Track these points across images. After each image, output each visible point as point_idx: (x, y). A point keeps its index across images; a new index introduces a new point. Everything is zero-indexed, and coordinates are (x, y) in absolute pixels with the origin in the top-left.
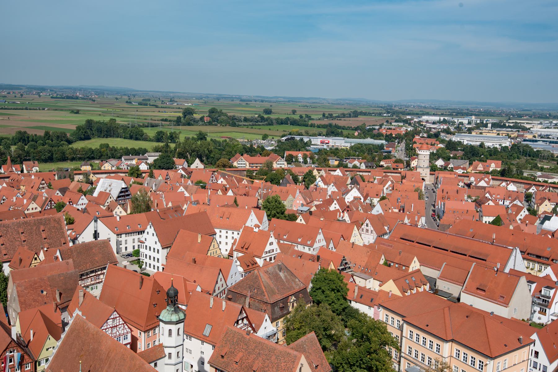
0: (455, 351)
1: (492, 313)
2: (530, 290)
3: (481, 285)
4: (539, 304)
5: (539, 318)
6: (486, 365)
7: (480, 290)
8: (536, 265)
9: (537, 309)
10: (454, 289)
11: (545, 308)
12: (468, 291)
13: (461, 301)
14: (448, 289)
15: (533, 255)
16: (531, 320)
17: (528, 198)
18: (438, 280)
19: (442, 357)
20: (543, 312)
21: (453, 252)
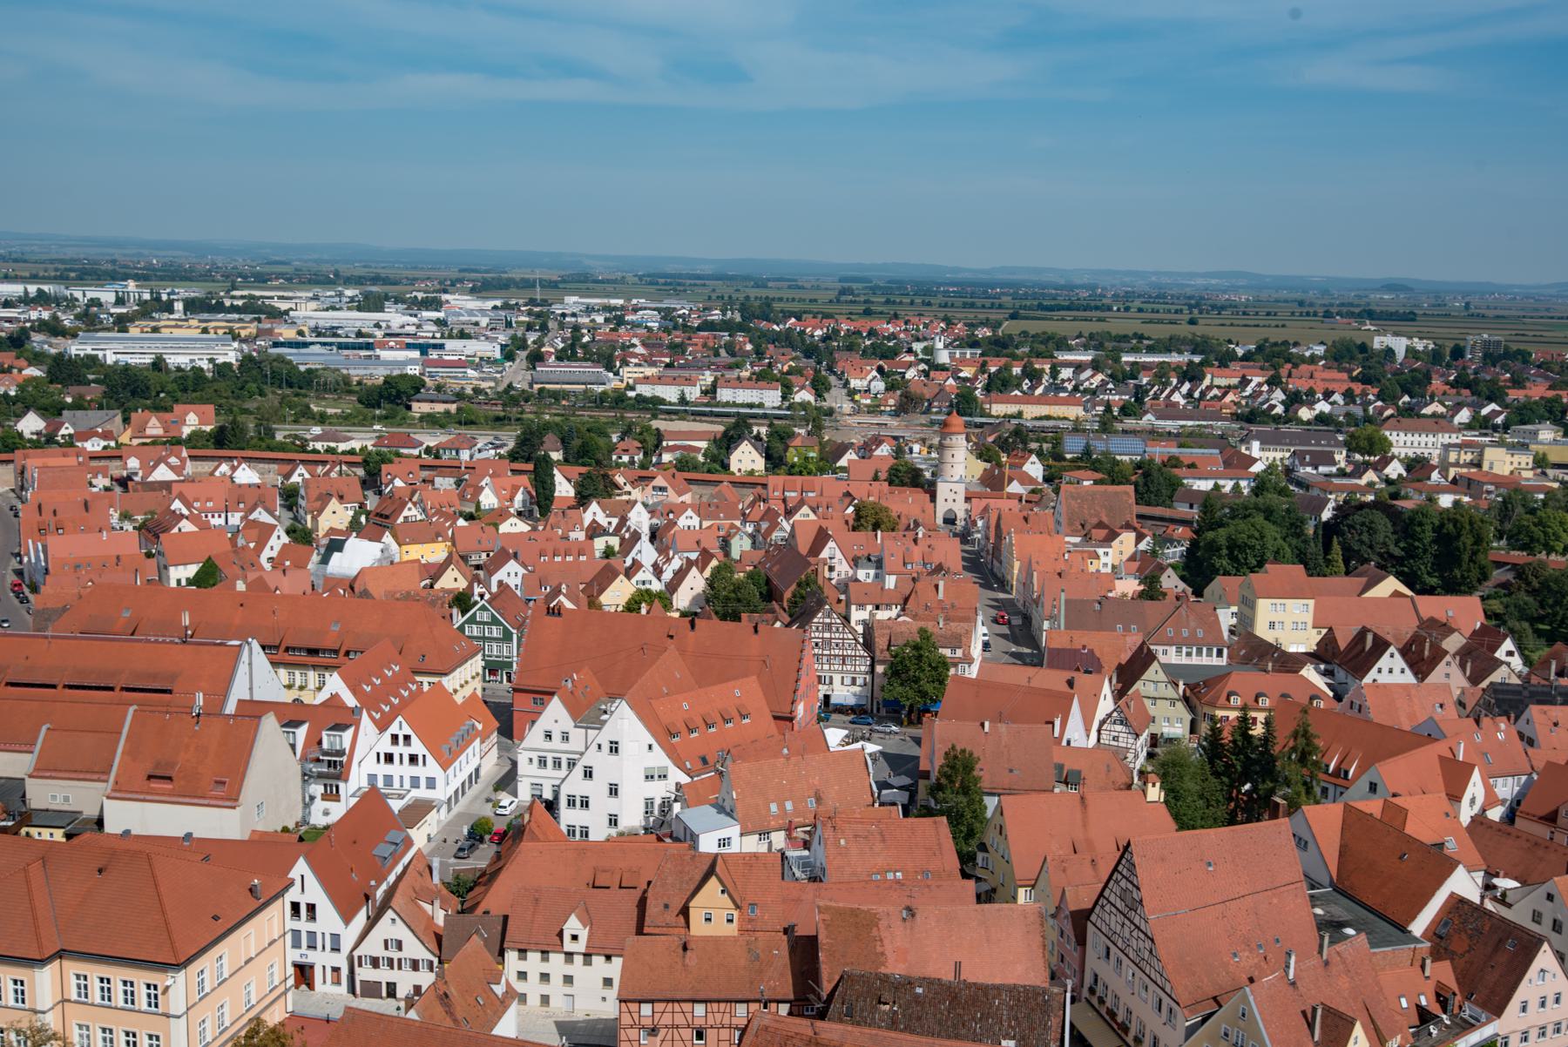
0: (74, 981)
1: (189, 836)
2: (293, 746)
3: (156, 767)
4: (320, 776)
5: (326, 813)
6: (167, 988)
7: (160, 780)
8: (312, 677)
9: (317, 789)
10: (79, 796)
11: (334, 782)
12: (122, 792)
13: (109, 827)
14: (66, 799)
15: (300, 649)
16: (305, 821)
17: (290, 497)
18: (29, 781)
19: (36, 1012)
20: (332, 795)
21: (70, 687)
